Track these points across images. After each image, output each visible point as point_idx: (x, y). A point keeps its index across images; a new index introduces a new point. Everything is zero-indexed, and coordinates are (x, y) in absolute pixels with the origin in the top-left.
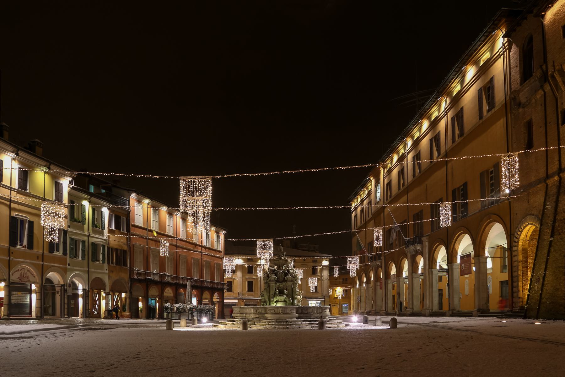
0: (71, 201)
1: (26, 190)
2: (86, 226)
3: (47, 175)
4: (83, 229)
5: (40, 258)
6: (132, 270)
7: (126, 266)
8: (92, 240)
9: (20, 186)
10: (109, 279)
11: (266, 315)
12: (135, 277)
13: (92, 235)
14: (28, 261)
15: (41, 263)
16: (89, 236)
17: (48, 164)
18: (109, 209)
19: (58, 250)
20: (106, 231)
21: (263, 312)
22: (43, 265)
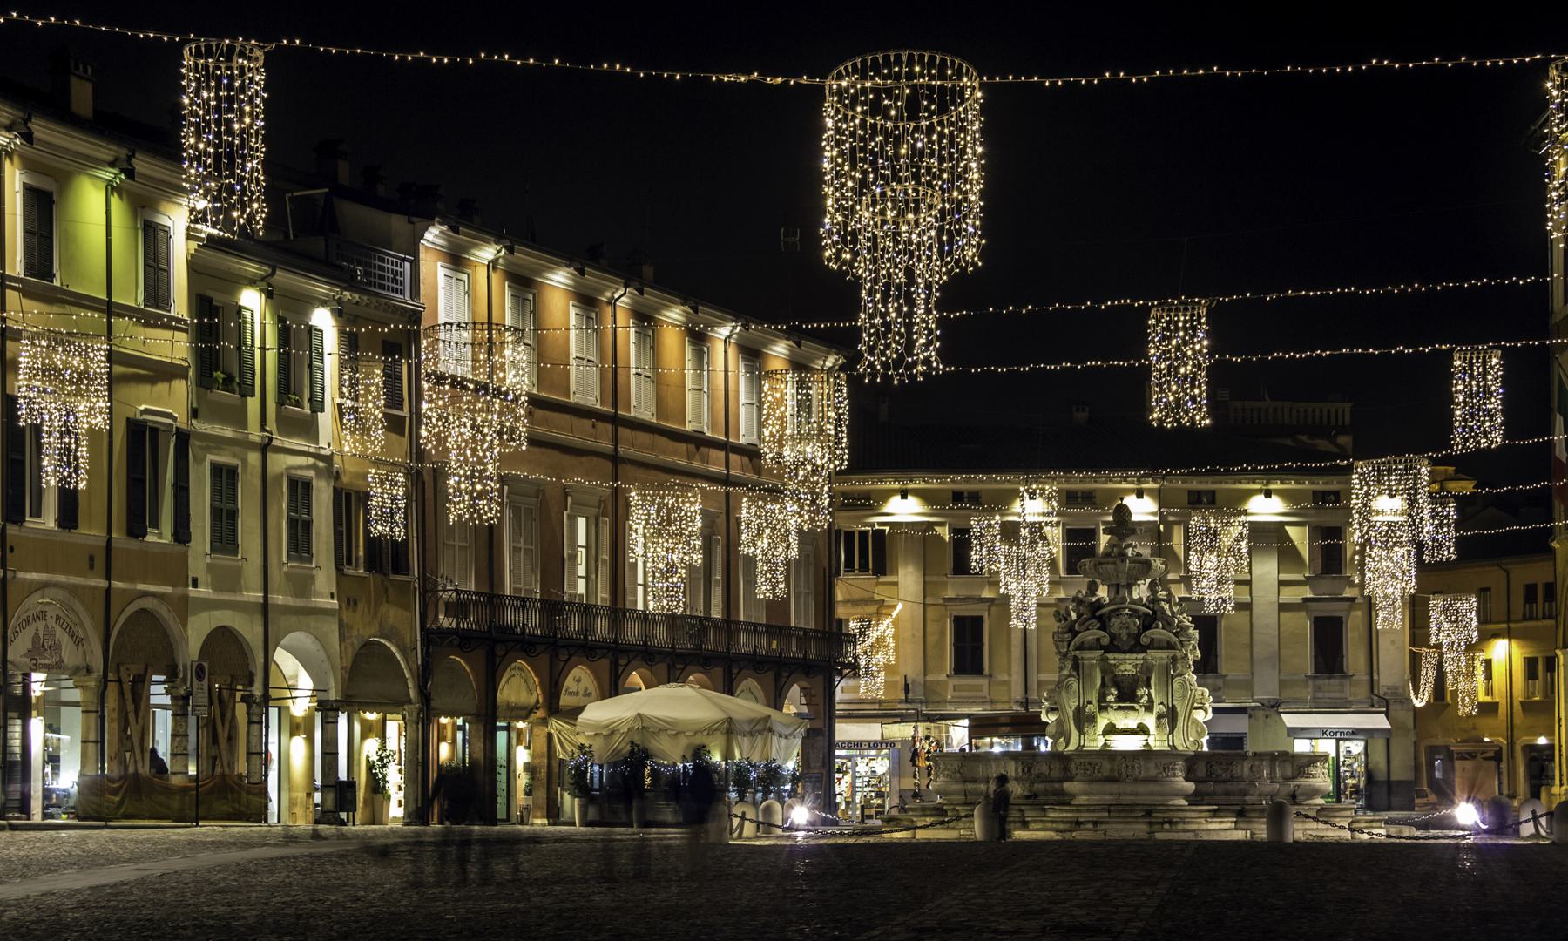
0: (202, 304)
1: (49, 276)
2: (253, 404)
3: (114, 199)
4: (240, 420)
5: (100, 562)
6: (428, 590)
7: (406, 570)
8: (280, 463)
9: (29, 268)
10: (342, 639)
11: (1067, 785)
12: (445, 622)
13: (279, 440)
14: (62, 578)
15: (103, 583)
16: (265, 448)
17: (124, 152)
18: (338, 314)
19: (156, 525)
20: (326, 420)
21: (1056, 774)
22: (108, 590)
